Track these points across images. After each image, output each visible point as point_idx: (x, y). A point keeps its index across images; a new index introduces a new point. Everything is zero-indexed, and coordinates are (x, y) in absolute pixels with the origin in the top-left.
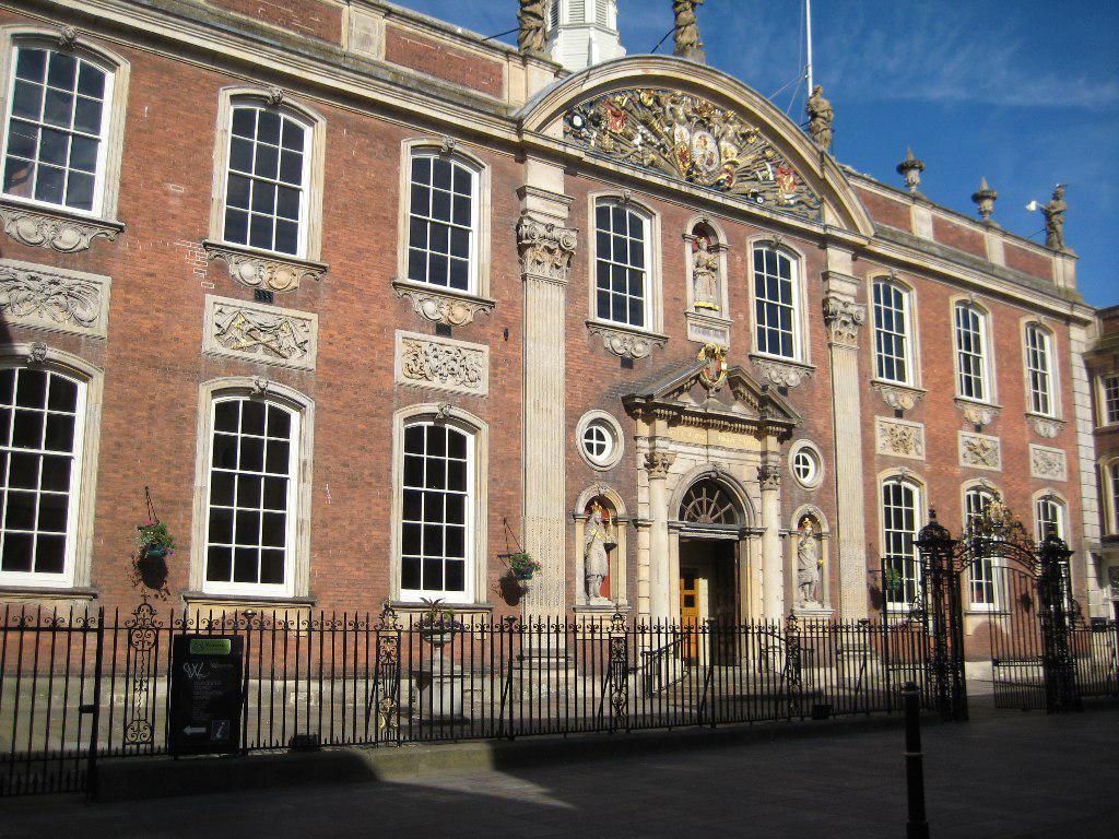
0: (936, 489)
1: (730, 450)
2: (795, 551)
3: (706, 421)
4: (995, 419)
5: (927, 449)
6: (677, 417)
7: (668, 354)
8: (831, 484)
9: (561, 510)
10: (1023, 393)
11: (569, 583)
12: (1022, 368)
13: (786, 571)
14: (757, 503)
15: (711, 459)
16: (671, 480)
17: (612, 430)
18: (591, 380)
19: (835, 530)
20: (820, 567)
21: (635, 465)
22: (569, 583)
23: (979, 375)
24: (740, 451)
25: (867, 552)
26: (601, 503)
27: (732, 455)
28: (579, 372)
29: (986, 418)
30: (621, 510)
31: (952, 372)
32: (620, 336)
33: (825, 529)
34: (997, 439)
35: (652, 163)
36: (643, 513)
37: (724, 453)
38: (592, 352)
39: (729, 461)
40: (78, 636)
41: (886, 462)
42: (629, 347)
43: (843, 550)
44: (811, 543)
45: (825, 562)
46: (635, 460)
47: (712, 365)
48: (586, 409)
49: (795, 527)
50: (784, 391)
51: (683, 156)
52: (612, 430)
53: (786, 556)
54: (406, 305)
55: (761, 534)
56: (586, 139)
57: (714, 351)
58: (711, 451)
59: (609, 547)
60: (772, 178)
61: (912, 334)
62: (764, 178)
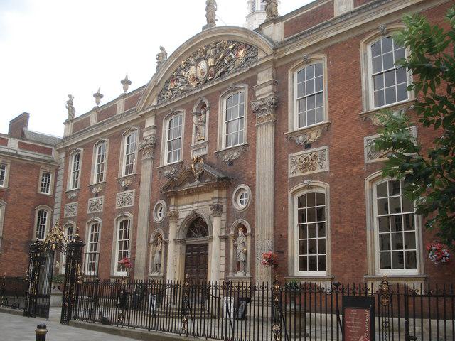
0: (339, 188)
1: (202, 202)
2: (232, 246)
3: (190, 193)
5: (331, 161)
6: (177, 195)
8: (252, 207)
11: (147, 268)
16: (180, 222)
19: (253, 232)
20: (246, 253)
22: (147, 268)
24: (207, 201)
26: (158, 239)
27: (203, 204)
33: (249, 231)
35: (183, 91)
40: (426, 299)
41: (296, 180)
48: (156, 203)
49: (232, 233)
50: (231, 163)
51: (194, 79)
54: (119, 184)
56: (164, 98)
60: (233, 57)
62: (229, 62)
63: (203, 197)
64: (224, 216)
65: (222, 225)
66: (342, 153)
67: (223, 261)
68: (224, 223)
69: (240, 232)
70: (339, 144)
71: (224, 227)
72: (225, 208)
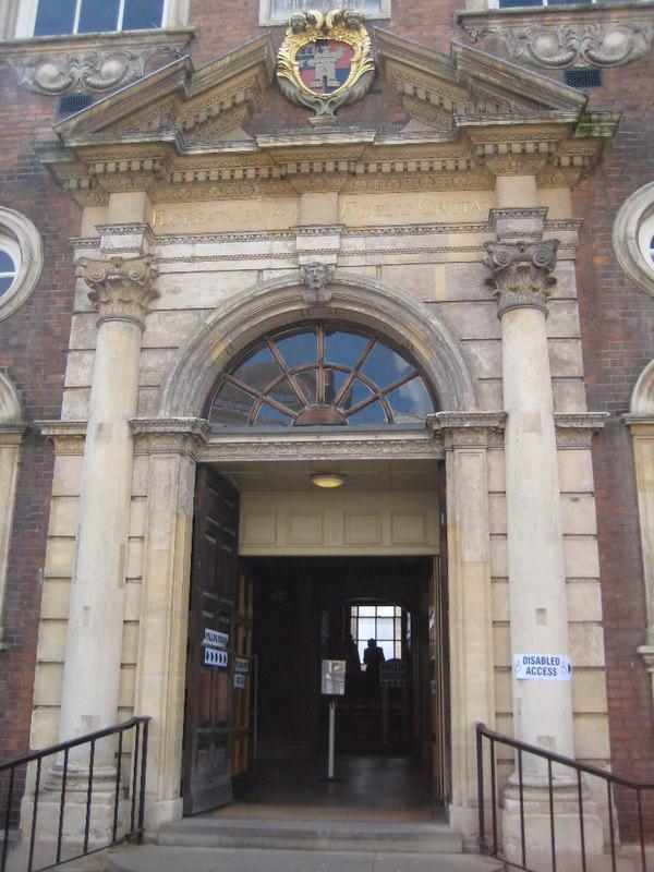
1: (370, 231)
14: (481, 355)
15: (303, 260)
21: (69, 307)
27: (387, 242)
36: (71, 409)
37: (357, 243)
39: (378, 259)
42: (78, 72)
46: (71, 294)
47: (325, 63)
50: (586, 78)
55: (500, 433)
57: (312, 20)
58: (302, 243)
63: (363, 207)
64: (568, 319)
65: (554, 361)
67: (588, 559)
68: (573, 353)
71: (577, 369)
72: (565, 271)
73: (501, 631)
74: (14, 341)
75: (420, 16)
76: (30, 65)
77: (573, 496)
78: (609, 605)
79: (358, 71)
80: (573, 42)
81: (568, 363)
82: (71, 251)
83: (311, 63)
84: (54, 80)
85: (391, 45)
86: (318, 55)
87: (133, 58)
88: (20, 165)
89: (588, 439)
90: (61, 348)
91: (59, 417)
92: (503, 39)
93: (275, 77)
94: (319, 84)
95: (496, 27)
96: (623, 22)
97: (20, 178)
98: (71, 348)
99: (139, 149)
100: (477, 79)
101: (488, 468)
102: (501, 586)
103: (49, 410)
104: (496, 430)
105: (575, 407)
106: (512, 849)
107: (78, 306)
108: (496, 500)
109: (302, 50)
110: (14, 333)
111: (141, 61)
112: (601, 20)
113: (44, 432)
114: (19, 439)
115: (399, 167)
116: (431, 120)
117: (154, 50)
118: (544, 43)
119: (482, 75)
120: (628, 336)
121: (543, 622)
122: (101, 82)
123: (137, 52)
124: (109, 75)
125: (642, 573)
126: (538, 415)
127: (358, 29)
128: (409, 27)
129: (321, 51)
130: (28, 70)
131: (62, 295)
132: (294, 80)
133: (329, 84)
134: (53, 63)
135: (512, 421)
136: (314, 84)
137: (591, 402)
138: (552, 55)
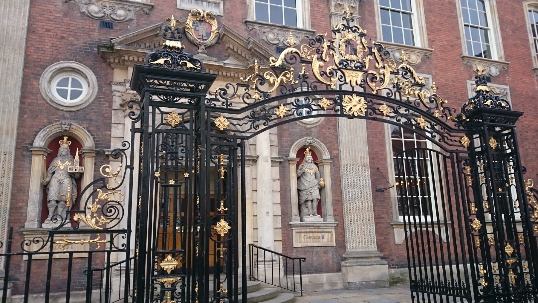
4: (503, 73)
7: (153, 18)
9: (10, 144)
10: (530, 54)
12: (527, 36)
13: (284, 192)
17: (86, 78)
18: (63, 38)
19: (335, 159)
20: (321, 189)
21: (110, 106)
23: (488, 43)
25: (372, 174)
28: (48, 30)
29: (494, 71)
30: (88, 143)
31: (459, 38)
32: (99, 4)
33: (326, 156)
34: (507, 87)
38: (66, 15)
42: (108, 12)
43: (344, 173)
44: (310, 168)
45: (328, 182)
46: (111, 102)
47: (202, 29)
48: (56, 60)
49: (293, 155)
52: (86, 78)
53: (284, 178)
55: (256, 161)
57: (200, 14)
59: (77, 178)
61: (417, 11)
65: (271, 141)
66: (446, 88)
67: (278, 198)
68: (275, 138)
69: (309, 156)
70: (442, 78)
71: (276, 143)
73: (255, 218)
74: (88, 117)
75: (232, 17)
76: (86, 4)
77: (274, 180)
78: (282, 211)
79: (212, 36)
80: (279, 37)
81: (274, 141)
82: (110, 84)
83: (197, 28)
84: (97, 13)
85: (229, 32)
86: (200, 26)
87: (129, 11)
88: (84, 46)
89: (278, 164)
90: (108, 121)
91: (110, 148)
92: (258, 31)
93: (185, 31)
94: (201, 37)
95: (257, 27)
96: (294, 33)
97: (85, 52)
98: (113, 122)
99: (142, 54)
100: (255, 50)
101: (252, 171)
102: (255, 205)
103: (105, 144)
104: (255, 160)
105: (275, 155)
106: (261, 278)
107: (114, 107)
108: (254, 180)
109: (194, 23)
110: (88, 114)
111: (133, 13)
112: (288, 31)
113: (106, 153)
114: (94, 155)
115: (228, 74)
116: (237, 58)
117: (138, 9)
118: (271, 36)
119: (258, 50)
120: (289, 134)
121: (268, 215)
122: (117, 18)
123: (131, 9)
124: (120, 16)
125: (291, 202)
126: (267, 157)
127: (214, 19)
128: (229, 21)
129: (201, 24)
130: (85, 6)
131: (106, 101)
132: (193, 35)
133: (205, 38)
134: (95, 5)
135: (260, 158)
136: (199, 37)
137: (279, 154)
138: (272, 41)
